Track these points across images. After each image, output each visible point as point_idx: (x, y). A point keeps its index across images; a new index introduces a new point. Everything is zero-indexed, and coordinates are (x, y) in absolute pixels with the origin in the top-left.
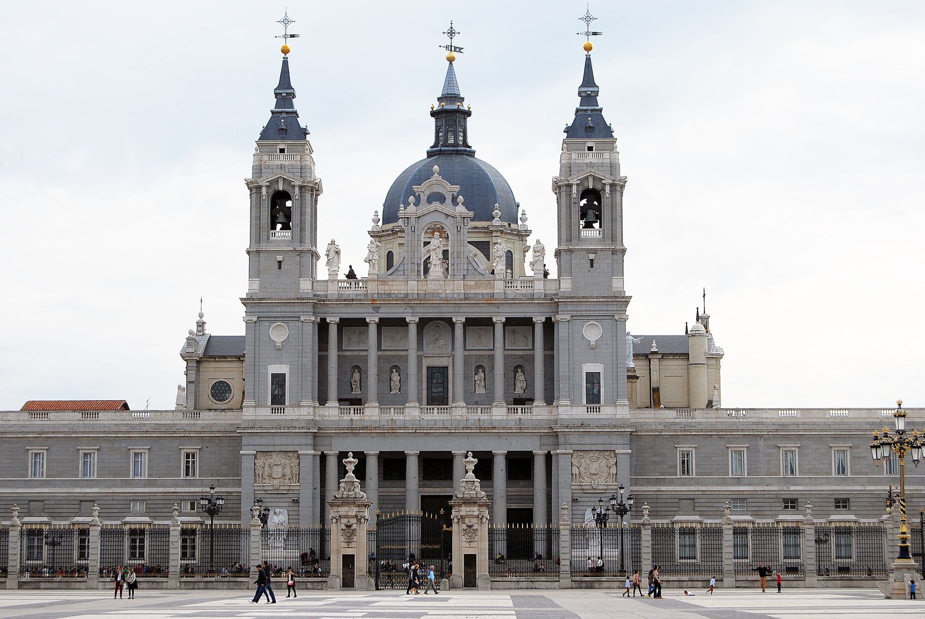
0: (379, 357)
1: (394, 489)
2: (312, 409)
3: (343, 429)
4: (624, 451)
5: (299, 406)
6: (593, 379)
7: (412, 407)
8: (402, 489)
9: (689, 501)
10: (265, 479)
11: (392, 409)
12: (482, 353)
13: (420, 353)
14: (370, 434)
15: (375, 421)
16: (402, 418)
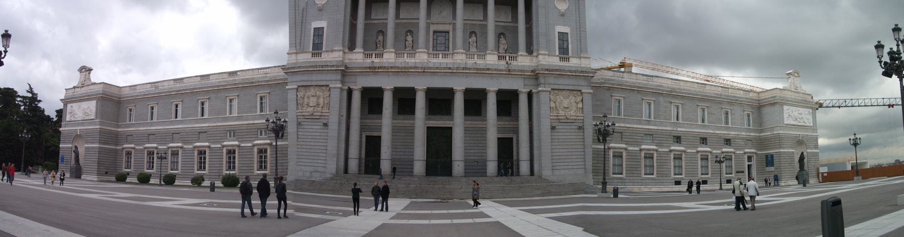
0: (397, 25)
1: (406, 122)
2: (341, 53)
3: (366, 69)
4: (588, 91)
5: (333, 51)
6: (563, 37)
7: (422, 52)
8: (412, 122)
9: (619, 134)
10: (304, 107)
11: (406, 55)
12: (475, 22)
13: (429, 21)
14: (387, 73)
15: (392, 63)
16: (413, 61)
